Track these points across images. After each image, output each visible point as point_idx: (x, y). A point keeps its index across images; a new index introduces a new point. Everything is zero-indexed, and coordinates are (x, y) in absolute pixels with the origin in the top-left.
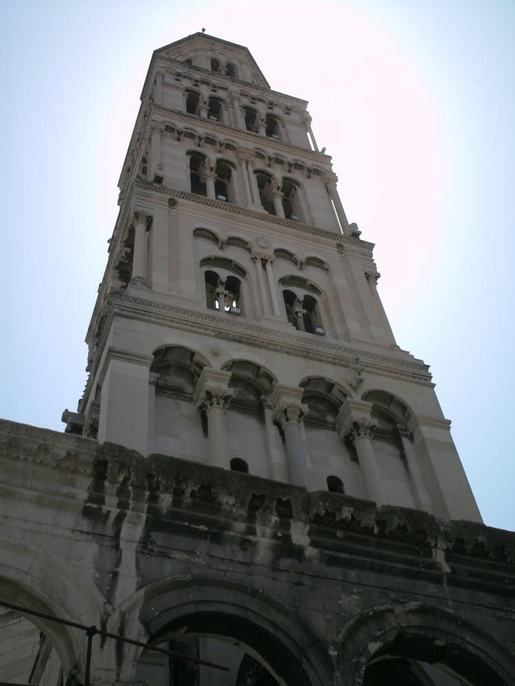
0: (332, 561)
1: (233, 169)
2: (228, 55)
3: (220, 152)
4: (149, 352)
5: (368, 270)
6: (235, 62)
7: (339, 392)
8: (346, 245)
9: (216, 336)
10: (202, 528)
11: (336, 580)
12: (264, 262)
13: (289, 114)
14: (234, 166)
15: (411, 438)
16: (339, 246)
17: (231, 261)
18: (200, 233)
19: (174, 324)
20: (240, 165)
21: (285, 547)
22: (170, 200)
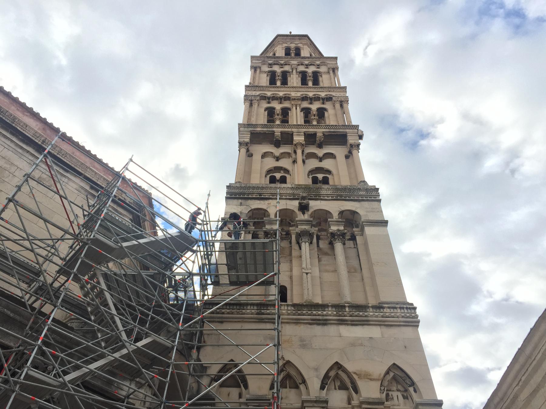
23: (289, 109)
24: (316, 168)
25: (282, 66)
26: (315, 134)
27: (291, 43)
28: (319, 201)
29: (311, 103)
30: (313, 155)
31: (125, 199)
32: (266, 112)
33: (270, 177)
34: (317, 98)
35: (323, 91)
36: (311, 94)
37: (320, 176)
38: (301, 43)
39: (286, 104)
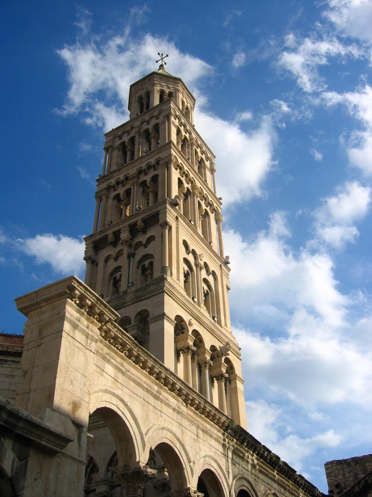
0: (260, 471)
1: (189, 196)
2: (188, 100)
3: (188, 184)
4: (173, 318)
5: (228, 284)
6: (189, 106)
7: (217, 354)
8: (223, 266)
9: (190, 315)
10: (241, 455)
11: (260, 479)
12: (201, 268)
13: (207, 161)
14: (190, 194)
15: (230, 382)
16: (221, 266)
17: (190, 262)
18: (185, 243)
19: (179, 303)
20: (194, 196)
21: (254, 466)
22: (177, 216)
23: (130, 189)
24: (143, 256)
25: (128, 132)
26: (135, 224)
27: (143, 89)
28: (124, 309)
29: (146, 175)
30: (139, 244)
31: (17, 350)
32: (115, 201)
33: (113, 279)
34: (149, 167)
35: (153, 157)
36: (144, 166)
37: (147, 263)
38: (150, 85)
39: (127, 186)
